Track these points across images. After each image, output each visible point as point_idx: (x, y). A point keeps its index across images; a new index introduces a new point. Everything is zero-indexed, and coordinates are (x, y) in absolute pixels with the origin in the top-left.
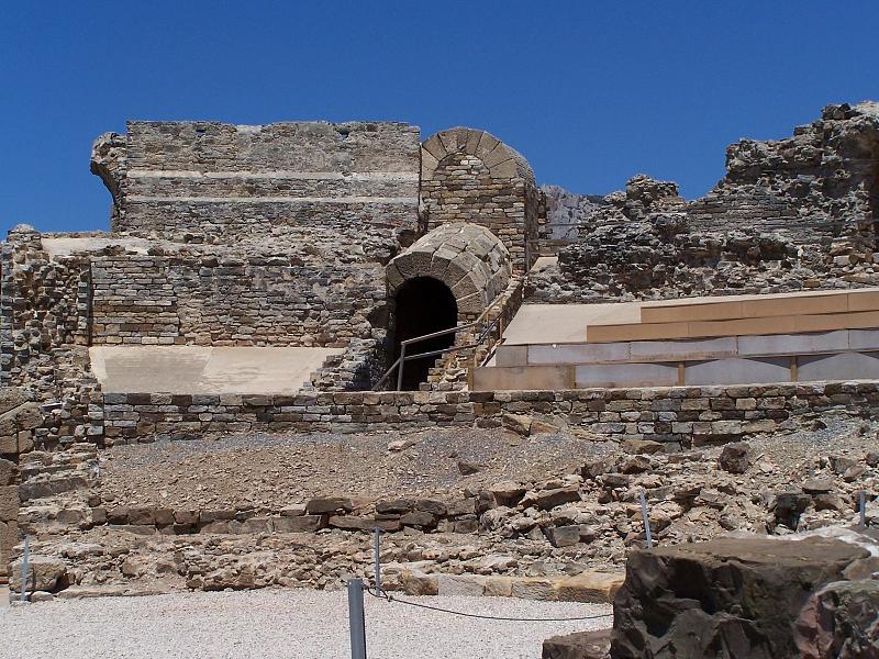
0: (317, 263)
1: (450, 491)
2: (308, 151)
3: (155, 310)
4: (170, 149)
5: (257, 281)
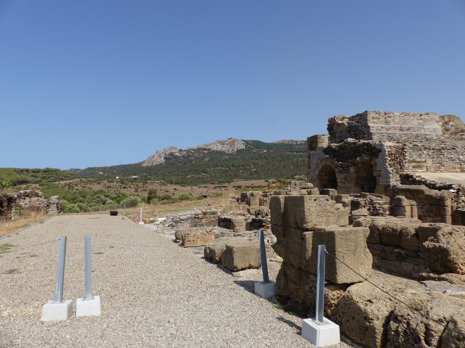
2: (412, 120)
4: (378, 118)
5: (445, 154)
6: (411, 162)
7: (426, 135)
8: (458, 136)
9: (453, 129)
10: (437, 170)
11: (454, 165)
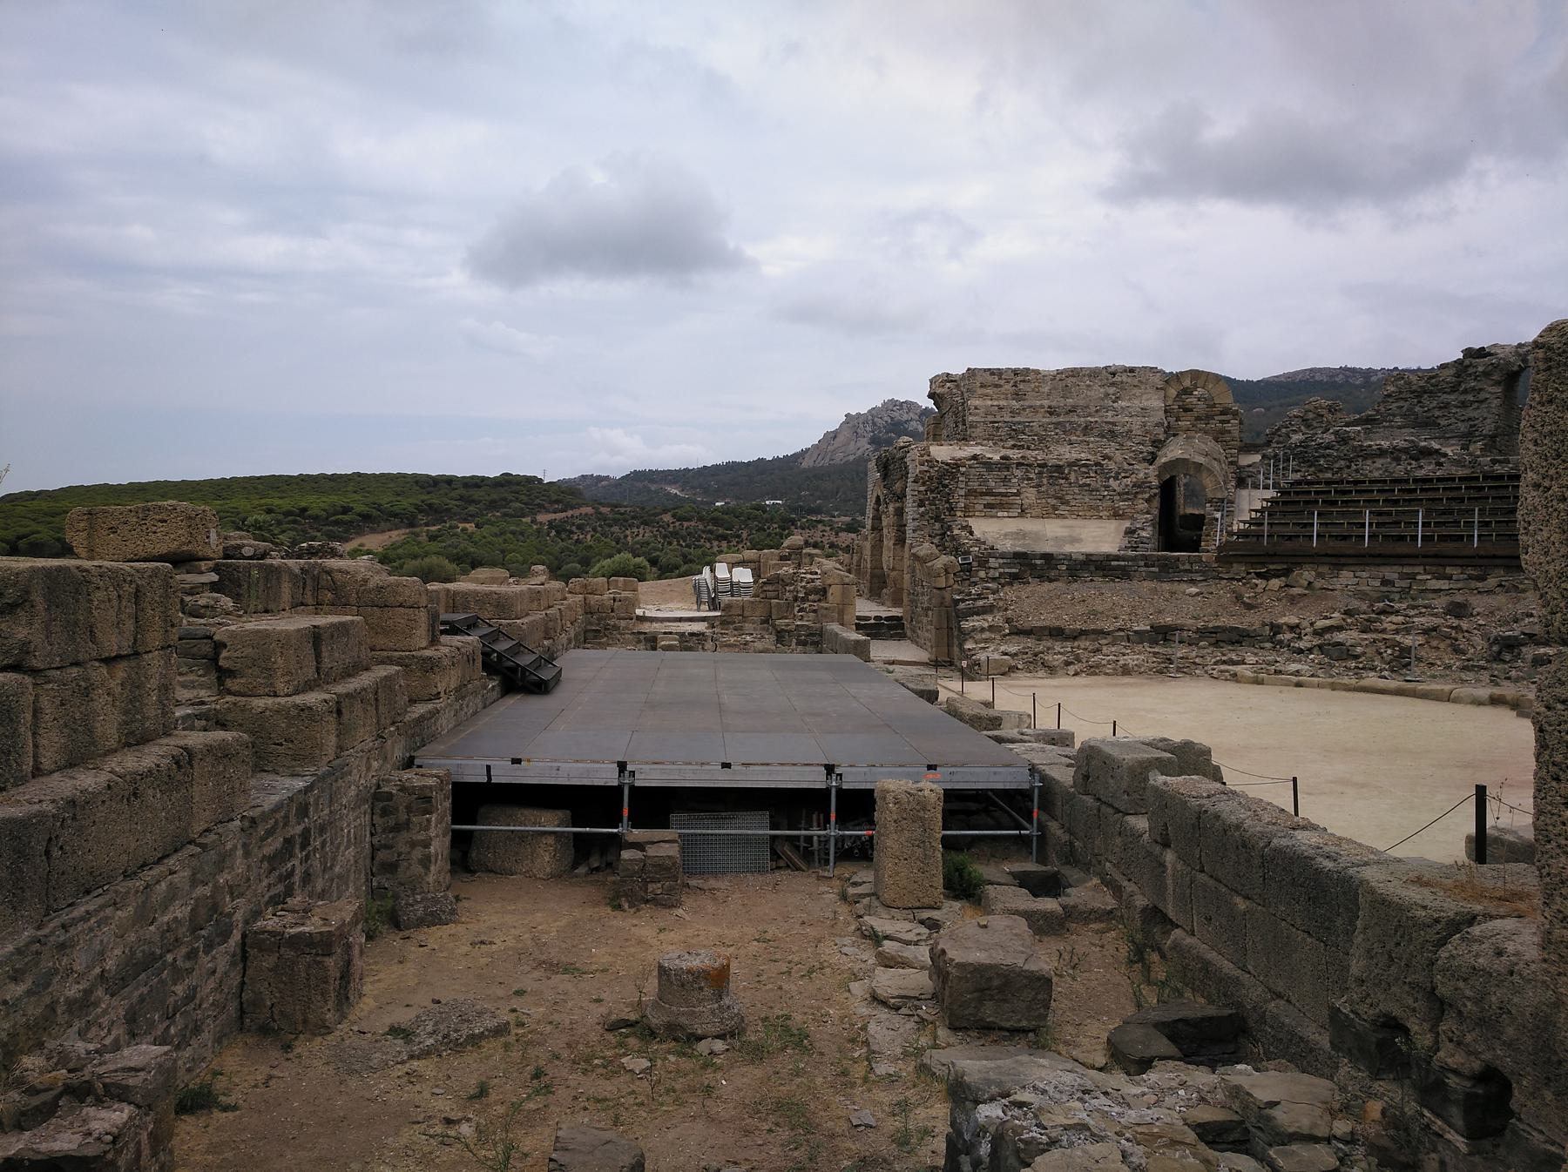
0: (1112, 466)
1: (1250, 621)
3: (1005, 495)
4: (996, 386)
5: (1072, 478)
6: (982, 494)
7: (1114, 424)
8: (1214, 424)
9: (1201, 408)
10: (1051, 512)
11: (1093, 503)
